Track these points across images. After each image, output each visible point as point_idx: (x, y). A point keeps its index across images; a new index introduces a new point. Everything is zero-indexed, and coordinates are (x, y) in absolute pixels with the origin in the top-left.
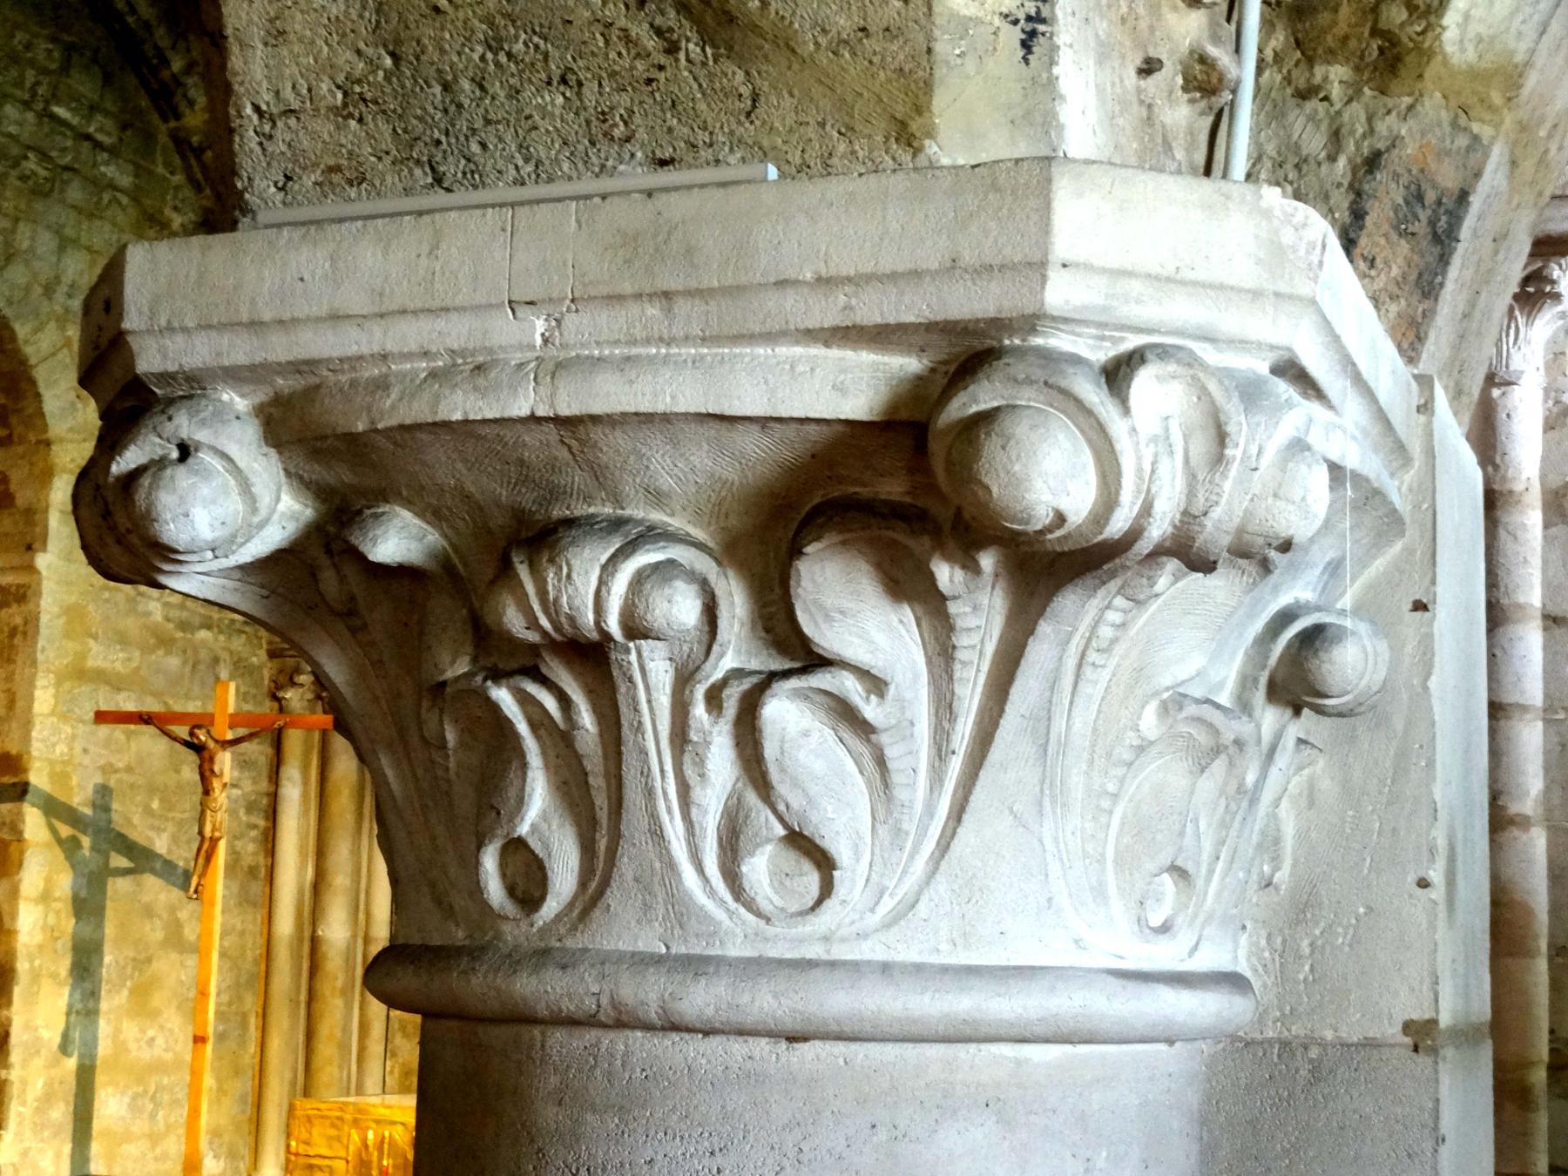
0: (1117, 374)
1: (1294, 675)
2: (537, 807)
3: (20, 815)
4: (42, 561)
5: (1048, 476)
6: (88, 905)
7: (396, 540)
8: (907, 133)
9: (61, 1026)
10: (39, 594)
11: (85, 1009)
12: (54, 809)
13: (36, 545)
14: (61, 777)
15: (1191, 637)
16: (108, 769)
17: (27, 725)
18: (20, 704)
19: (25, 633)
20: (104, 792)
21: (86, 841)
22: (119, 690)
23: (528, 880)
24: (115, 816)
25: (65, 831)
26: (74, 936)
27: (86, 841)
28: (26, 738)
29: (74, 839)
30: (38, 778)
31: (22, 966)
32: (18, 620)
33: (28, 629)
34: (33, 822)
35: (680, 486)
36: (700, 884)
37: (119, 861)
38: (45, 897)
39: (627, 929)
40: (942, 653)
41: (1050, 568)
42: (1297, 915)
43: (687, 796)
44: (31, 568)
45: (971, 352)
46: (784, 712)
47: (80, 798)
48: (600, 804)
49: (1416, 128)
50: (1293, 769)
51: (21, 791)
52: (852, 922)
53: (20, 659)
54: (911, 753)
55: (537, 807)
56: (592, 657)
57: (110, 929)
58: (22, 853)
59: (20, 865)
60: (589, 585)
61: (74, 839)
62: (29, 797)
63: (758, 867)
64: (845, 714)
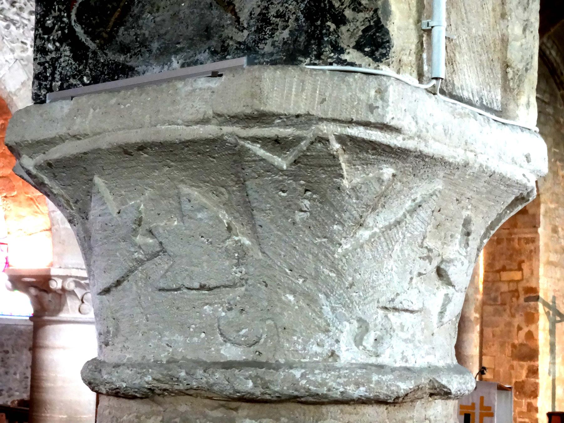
3: (537, 305)
4: (540, 230)
6: (552, 332)
9: (548, 368)
10: (539, 240)
11: (553, 363)
12: (545, 304)
13: (537, 226)
14: (546, 294)
16: (555, 291)
17: (538, 279)
18: (535, 273)
19: (535, 252)
20: (554, 297)
21: (551, 312)
22: (556, 267)
24: (557, 305)
25: (547, 310)
26: (550, 340)
27: (551, 312)
28: (538, 283)
29: (548, 312)
30: (541, 295)
31: (540, 350)
32: (533, 248)
33: (536, 250)
34: (541, 308)
37: (558, 319)
38: (544, 330)
44: (537, 232)
47: (549, 300)
51: (537, 298)
53: (534, 259)
57: (557, 339)
58: (538, 316)
59: (538, 319)
61: (548, 312)
62: (540, 300)
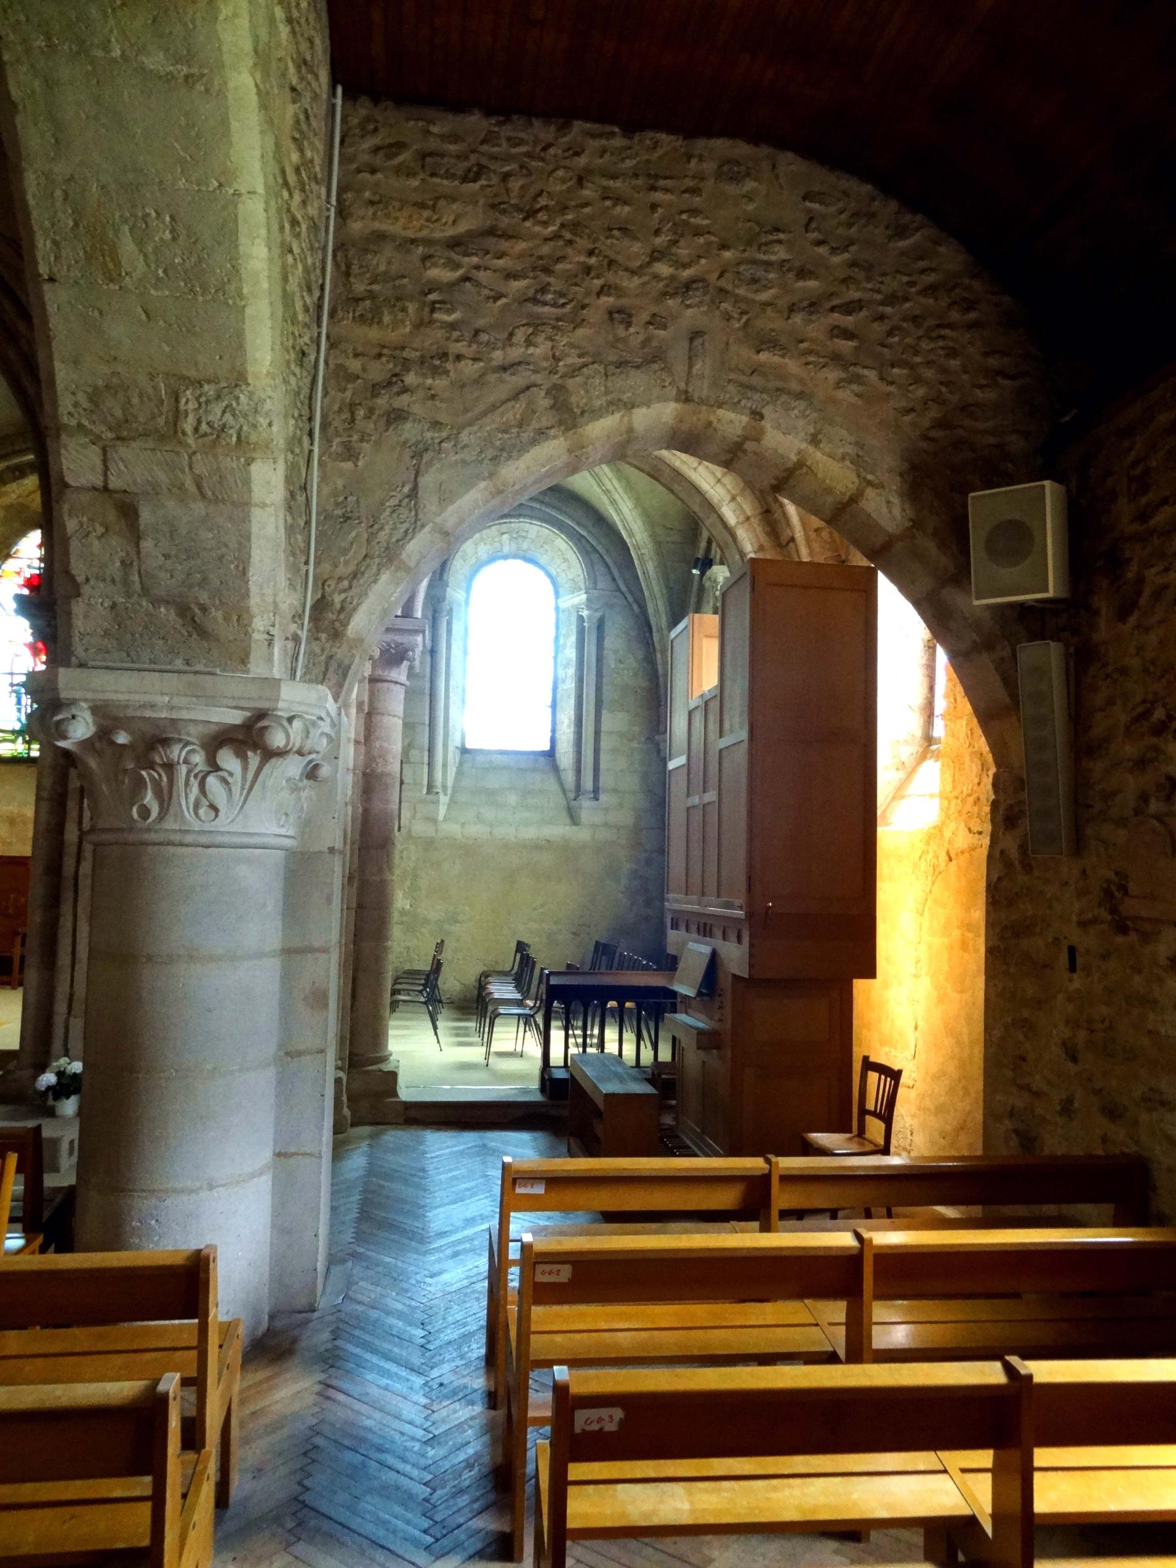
0: (290, 720)
1: (312, 773)
2: (149, 798)
5: (277, 739)
7: (122, 738)
8: (244, 661)
15: (293, 767)
23: (145, 812)
35: (193, 733)
36: (189, 815)
39: (170, 824)
40: (245, 769)
41: (270, 754)
42: (307, 825)
43: (186, 796)
45: (261, 715)
46: (211, 780)
48: (165, 798)
49: (341, 652)
50: (308, 792)
52: (223, 823)
54: (236, 790)
55: (149, 798)
56: (170, 767)
60: (176, 752)
63: (202, 812)
64: (224, 781)
